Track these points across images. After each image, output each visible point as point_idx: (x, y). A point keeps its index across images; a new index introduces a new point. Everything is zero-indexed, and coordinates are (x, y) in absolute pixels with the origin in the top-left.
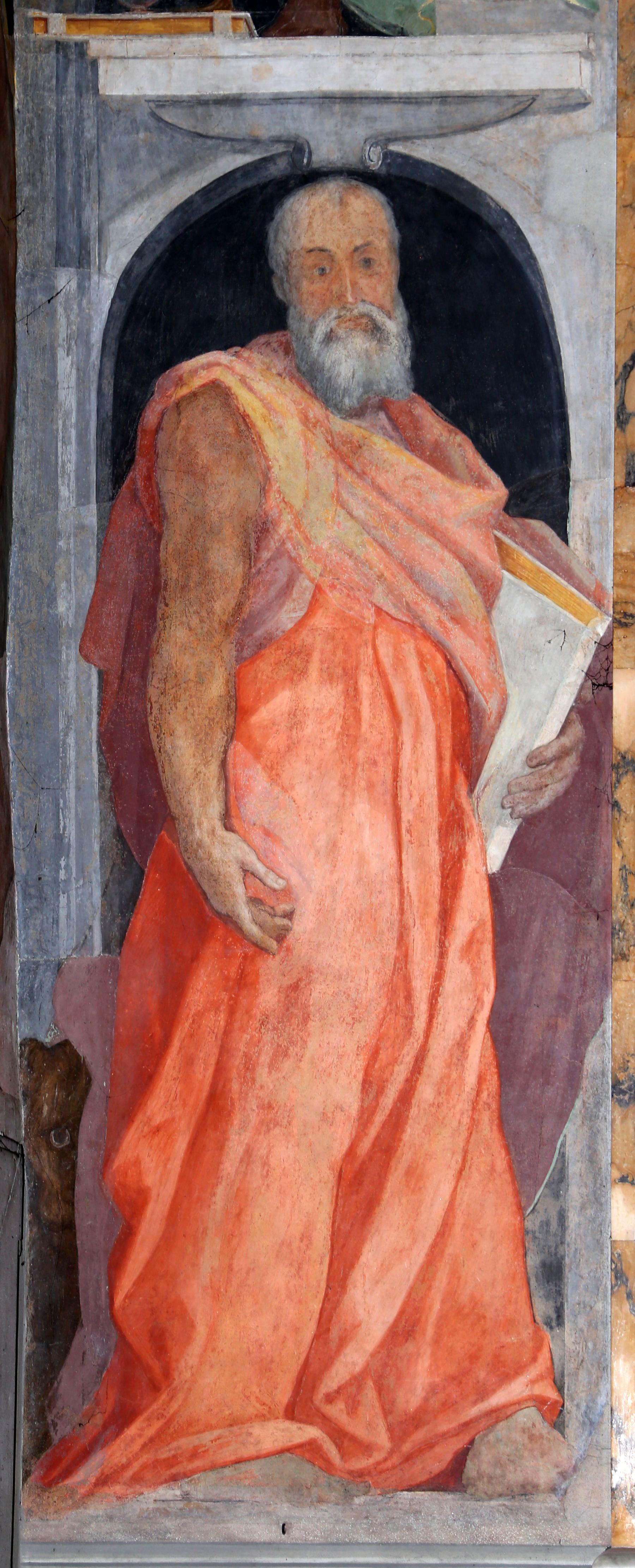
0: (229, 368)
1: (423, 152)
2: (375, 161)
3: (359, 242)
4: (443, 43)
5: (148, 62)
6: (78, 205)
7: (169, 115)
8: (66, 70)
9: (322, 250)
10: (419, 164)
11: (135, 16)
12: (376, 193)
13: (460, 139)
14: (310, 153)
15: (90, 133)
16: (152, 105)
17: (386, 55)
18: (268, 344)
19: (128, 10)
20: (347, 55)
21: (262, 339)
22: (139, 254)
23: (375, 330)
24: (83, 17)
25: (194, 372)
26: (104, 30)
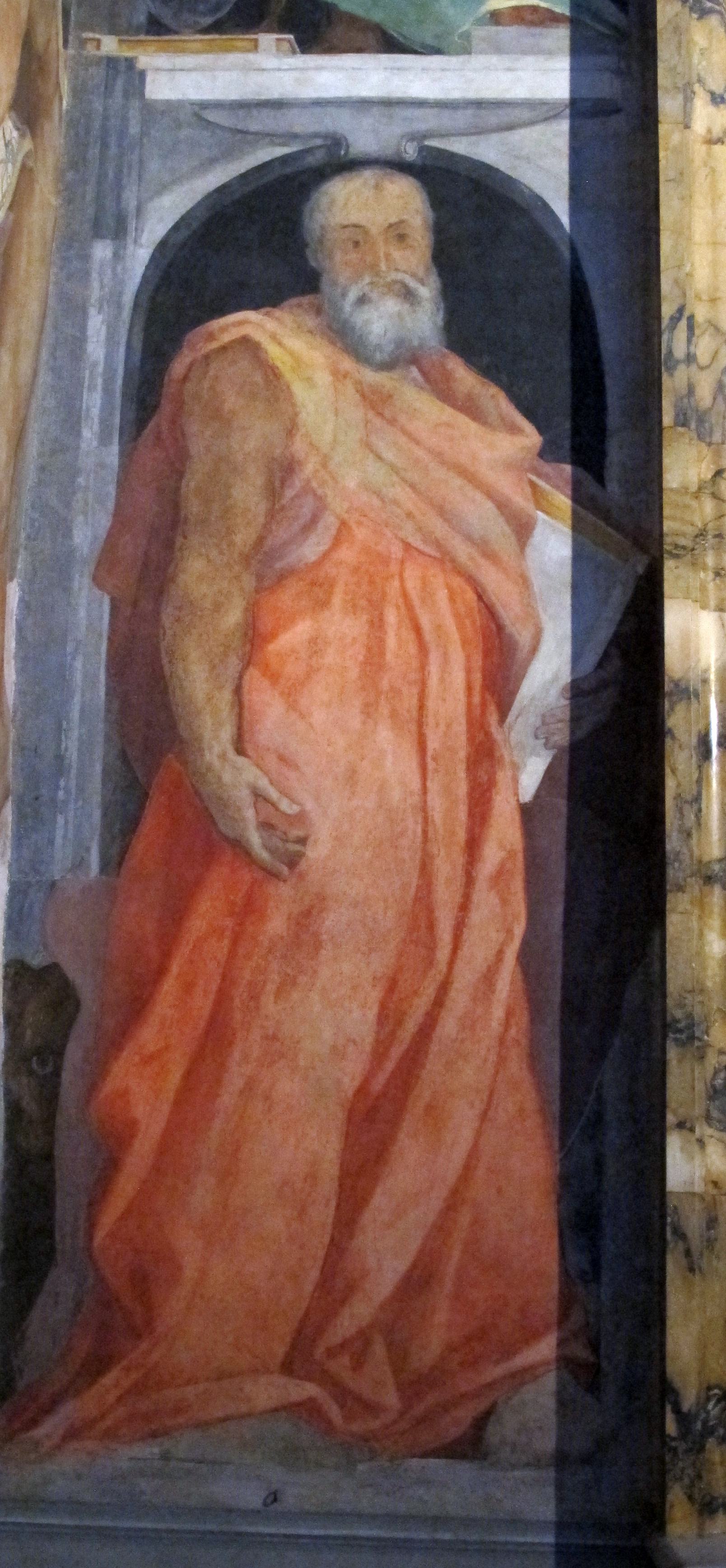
0: (260, 326)
1: (459, 146)
2: (411, 152)
3: (393, 219)
4: (477, 61)
5: (194, 75)
6: (119, 186)
7: (211, 116)
8: (114, 79)
9: (356, 226)
10: (452, 155)
11: (183, 38)
12: (411, 180)
13: (495, 138)
14: (348, 146)
15: (134, 129)
16: (197, 108)
17: (423, 69)
18: (299, 306)
19: (176, 33)
20: (386, 69)
21: (294, 301)
22: (176, 228)
23: (408, 295)
24: (132, 38)
25: (223, 329)
26: (153, 48)
